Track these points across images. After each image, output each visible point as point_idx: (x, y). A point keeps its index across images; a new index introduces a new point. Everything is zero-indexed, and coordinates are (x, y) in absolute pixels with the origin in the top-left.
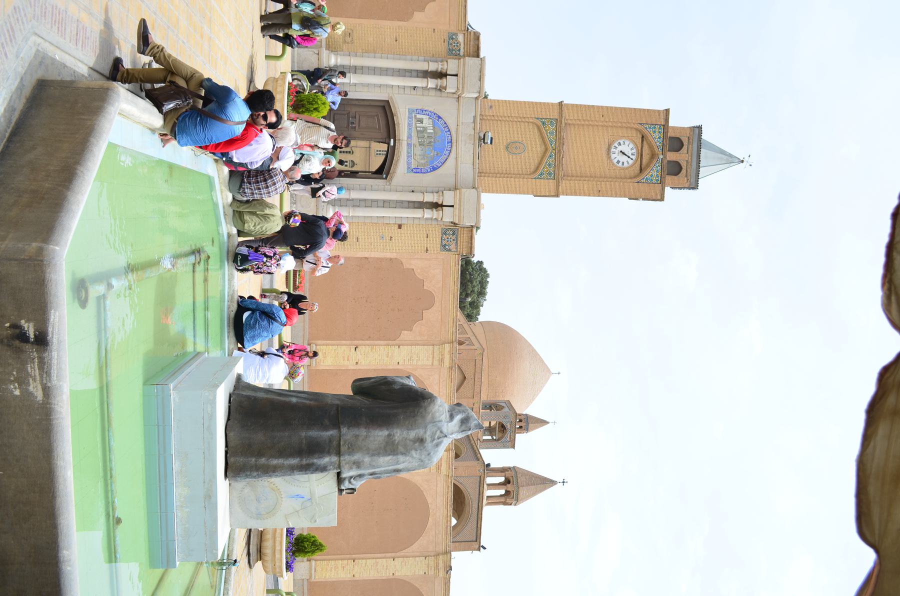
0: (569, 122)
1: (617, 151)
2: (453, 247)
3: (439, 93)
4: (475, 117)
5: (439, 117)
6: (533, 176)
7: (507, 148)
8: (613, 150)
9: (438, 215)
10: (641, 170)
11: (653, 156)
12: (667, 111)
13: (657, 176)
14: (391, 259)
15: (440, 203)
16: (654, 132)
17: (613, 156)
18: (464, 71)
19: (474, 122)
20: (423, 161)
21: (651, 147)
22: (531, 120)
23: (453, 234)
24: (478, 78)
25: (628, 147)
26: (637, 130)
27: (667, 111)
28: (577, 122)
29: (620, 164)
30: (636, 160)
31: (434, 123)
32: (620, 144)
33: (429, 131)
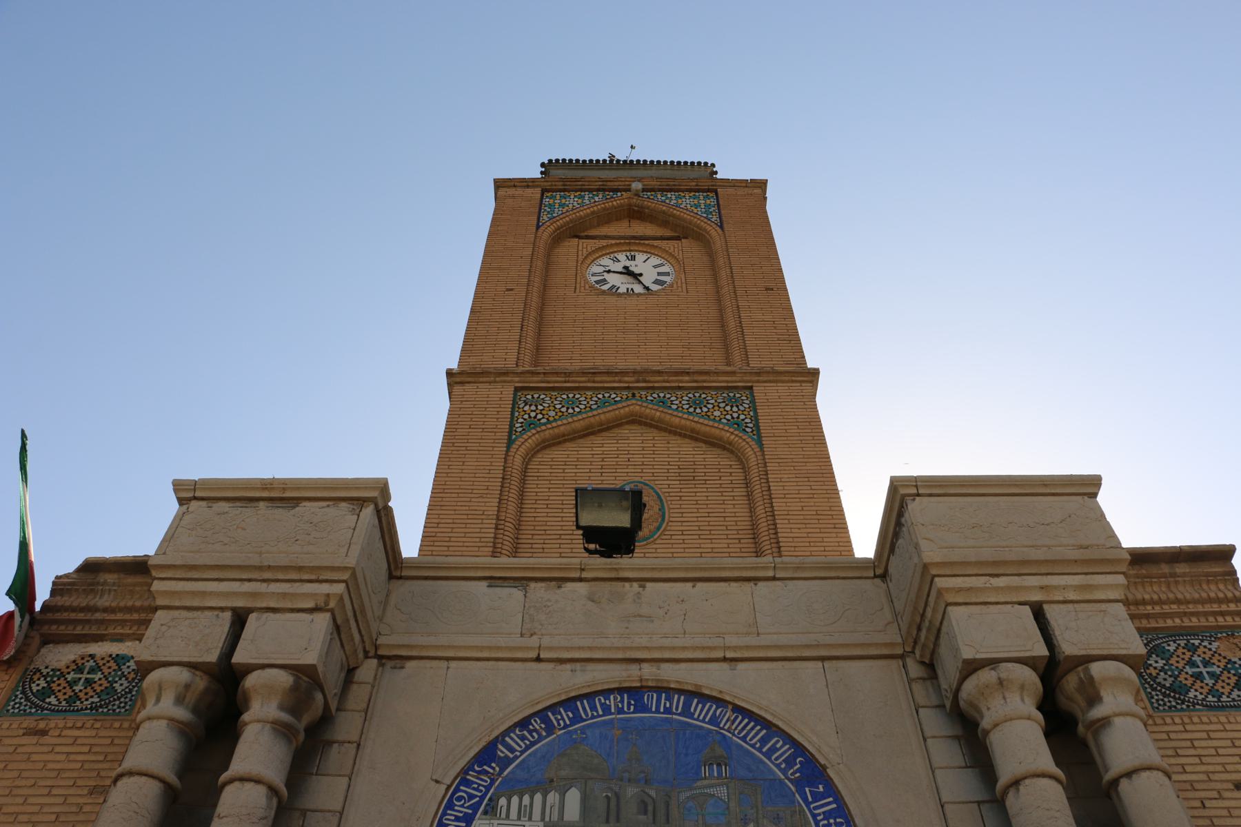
3: (336, 757)
4: (493, 581)
5: (487, 755)
6: (751, 453)
9: (1117, 681)
10: (678, 238)
11: (635, 214)
18: (221, 571)
19: (522, 582)
21: (607, 217)
24: (280, 513)
25: (607, 270)
26: (558, 238)
27: (500, 184)
30: (651, 251)
31: (514, 787)
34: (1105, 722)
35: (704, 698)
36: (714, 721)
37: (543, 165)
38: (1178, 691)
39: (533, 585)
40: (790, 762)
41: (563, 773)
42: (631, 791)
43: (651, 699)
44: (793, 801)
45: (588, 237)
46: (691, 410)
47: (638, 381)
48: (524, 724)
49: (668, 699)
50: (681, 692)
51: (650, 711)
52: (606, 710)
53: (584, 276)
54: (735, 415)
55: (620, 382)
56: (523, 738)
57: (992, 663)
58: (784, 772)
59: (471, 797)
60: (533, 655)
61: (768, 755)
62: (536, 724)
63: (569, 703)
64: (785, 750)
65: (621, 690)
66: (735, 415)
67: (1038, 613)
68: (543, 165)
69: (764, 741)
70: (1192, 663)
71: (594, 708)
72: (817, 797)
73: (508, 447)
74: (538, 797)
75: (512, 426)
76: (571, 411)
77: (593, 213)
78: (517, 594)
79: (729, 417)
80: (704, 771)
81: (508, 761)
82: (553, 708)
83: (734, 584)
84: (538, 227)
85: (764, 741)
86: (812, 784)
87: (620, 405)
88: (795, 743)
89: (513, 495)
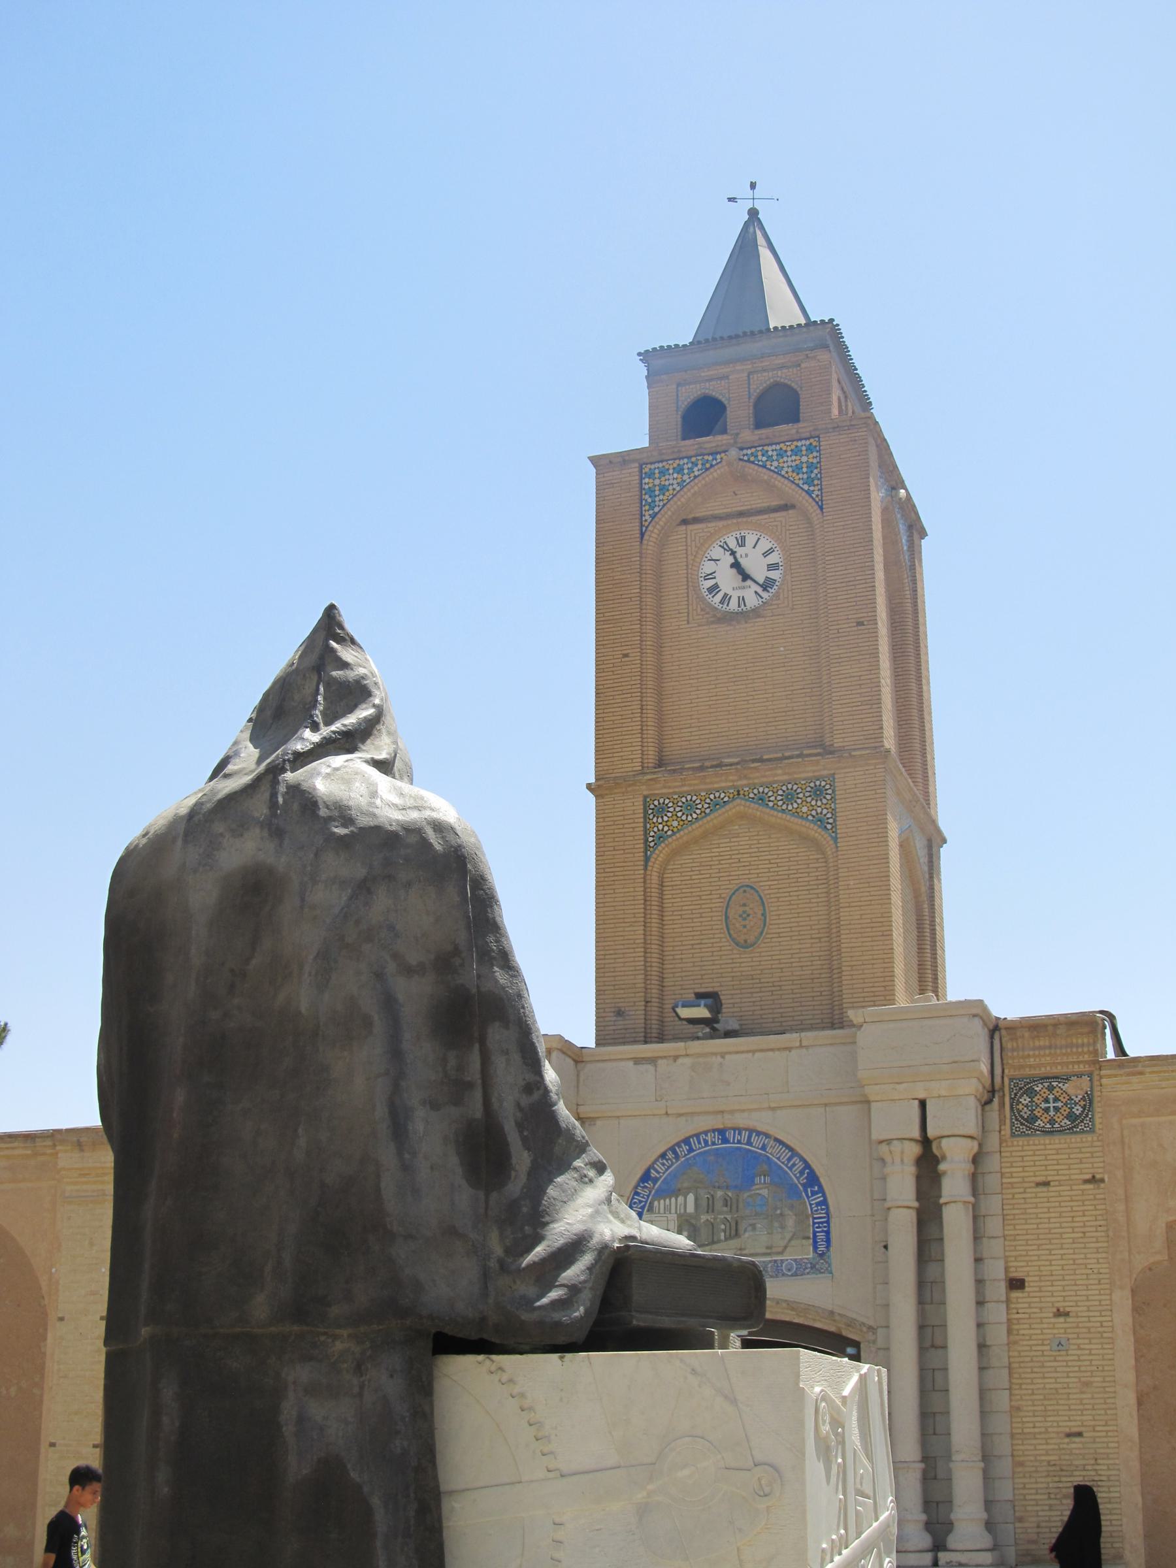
0: (652, 755)
1: (735, 595)
2: (1075, 1089)
4: (638, 1061)
5: (646, 1177)
7: (746, 945)
8: (733, 605)
10: (785, 507)
12: (595, 460)
13: (797, 452)
14: (1136, 1310)
15: (915, 1150)
16: (663, 489)
17: (752, 601)
19: (653, 1061)
20: (790, 1222)
22: (655, 878)
23: (1031, 1093)
27: (595, 460)
28: (651, 732)
29: (775, 575)
31: (662, 1194)
32: (714, 589)
33: (691, 1209)
34: (945, 1173)
35: (759, 1133)
36: (764, 1148)
37: (639, 354)
38: (1032, 1119)
39: (660, 1062)
40: (802, 1173)
41: (686, 1185)
42: (719, 1193)
43: (730, 1135)
44: (801, 1196)
45: (696, 520)
46: (784, 807)
47: (740, 779)
48: (663, 1156)
49: (740, 1134)
50: (746, 1129)
51: (728, 1142)
52: (706, 1142)
53: (697, 588)
54: (819, 810)
55: (726, 781)
56: (663, 1164)
57: (889, 1142)
58: (798, 1179)
59: (640, 1202)
60: (664, 1112)
61: (791, 1169)
62: (670, 1155)
63: (686, 1141)
64: (800, 1165)
65: (714, 1131)
66: (819, 810)
67: (923, 1104)
68: (639, 354)
69: (789, 1159)
70: (1046, 1101)
71: (699, 1143)
72: (813, 1193)
73: (645, 869)
74: (673, 1199)
75: (646, 840)
76: (690, 818)
77: (694, 494)
78: (650, 1068)
79: (814, 813)
80: (757, 1180)
81: (655, 1180)
82: (678, 1144)
83: (777, 1053)
84: (642, 535)
85: (789, 1159)
86: (812, 1186)
87: (727, 807)
88: (805, 1162)
89: (655, 920)
